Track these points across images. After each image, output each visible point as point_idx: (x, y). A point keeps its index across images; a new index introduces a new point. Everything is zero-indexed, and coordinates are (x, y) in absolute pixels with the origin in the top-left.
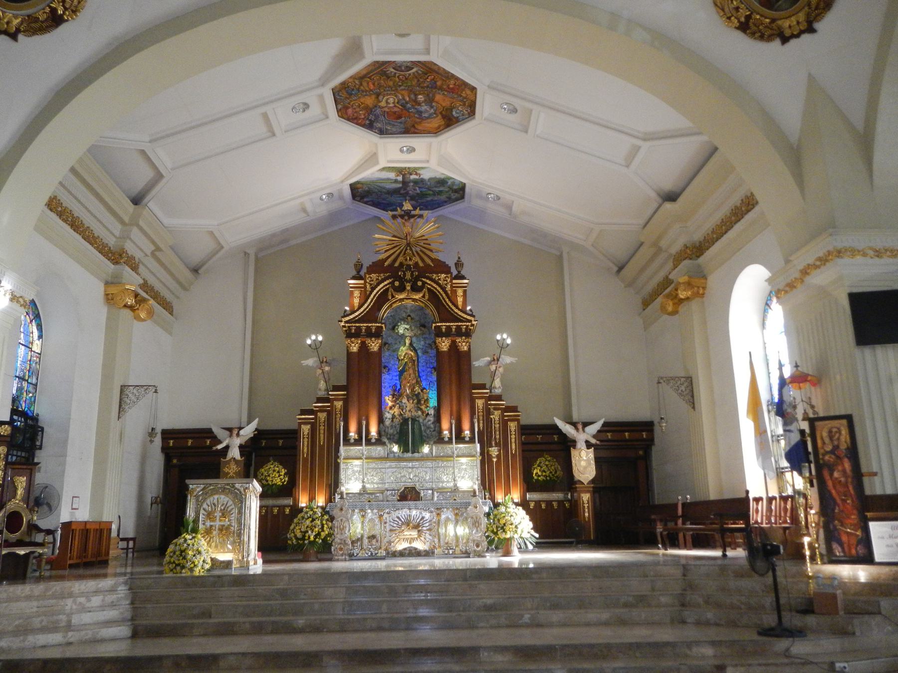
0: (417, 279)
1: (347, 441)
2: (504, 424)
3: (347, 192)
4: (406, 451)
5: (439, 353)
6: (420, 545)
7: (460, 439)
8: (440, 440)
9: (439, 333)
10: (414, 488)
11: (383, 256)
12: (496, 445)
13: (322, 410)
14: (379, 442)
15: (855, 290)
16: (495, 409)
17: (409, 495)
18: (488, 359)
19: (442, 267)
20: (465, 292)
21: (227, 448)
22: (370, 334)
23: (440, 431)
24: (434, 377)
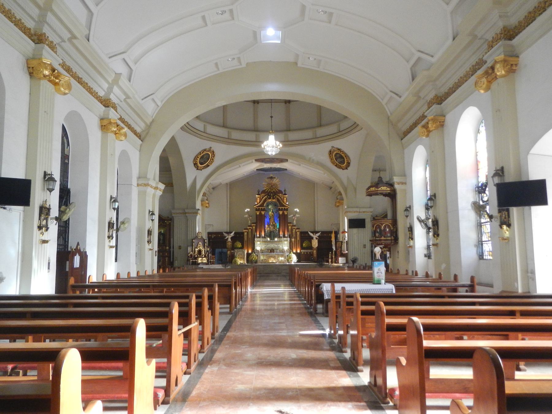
0: (274, 196)
1: (257, 238)
2: (296, 232)
3: (255, 170)
4: (271, 239)
5: (279, 214)
6: (274, 261)
7: (284, 236)
8: (279, 237)
9: (279, 210)
10: (273, 249)
11: (265, 189)
12: (294, 238)
13: (250, 229)
14: (264, 237)
15: (350, 218)
16: (294, 229)
17: (272, 251)
18: (292, 215)
19: (280, 192)
20: (286, 198)
21: (228, 238)
22: (262, 210)
23: (280, 235)
24: (278, 219)
